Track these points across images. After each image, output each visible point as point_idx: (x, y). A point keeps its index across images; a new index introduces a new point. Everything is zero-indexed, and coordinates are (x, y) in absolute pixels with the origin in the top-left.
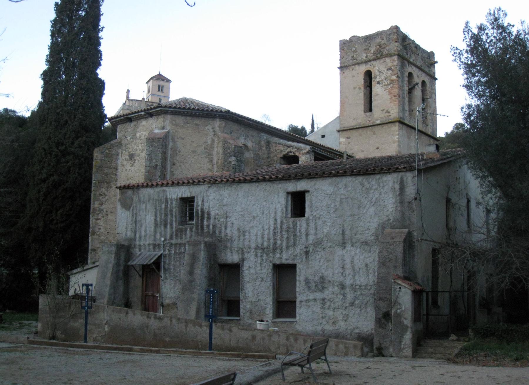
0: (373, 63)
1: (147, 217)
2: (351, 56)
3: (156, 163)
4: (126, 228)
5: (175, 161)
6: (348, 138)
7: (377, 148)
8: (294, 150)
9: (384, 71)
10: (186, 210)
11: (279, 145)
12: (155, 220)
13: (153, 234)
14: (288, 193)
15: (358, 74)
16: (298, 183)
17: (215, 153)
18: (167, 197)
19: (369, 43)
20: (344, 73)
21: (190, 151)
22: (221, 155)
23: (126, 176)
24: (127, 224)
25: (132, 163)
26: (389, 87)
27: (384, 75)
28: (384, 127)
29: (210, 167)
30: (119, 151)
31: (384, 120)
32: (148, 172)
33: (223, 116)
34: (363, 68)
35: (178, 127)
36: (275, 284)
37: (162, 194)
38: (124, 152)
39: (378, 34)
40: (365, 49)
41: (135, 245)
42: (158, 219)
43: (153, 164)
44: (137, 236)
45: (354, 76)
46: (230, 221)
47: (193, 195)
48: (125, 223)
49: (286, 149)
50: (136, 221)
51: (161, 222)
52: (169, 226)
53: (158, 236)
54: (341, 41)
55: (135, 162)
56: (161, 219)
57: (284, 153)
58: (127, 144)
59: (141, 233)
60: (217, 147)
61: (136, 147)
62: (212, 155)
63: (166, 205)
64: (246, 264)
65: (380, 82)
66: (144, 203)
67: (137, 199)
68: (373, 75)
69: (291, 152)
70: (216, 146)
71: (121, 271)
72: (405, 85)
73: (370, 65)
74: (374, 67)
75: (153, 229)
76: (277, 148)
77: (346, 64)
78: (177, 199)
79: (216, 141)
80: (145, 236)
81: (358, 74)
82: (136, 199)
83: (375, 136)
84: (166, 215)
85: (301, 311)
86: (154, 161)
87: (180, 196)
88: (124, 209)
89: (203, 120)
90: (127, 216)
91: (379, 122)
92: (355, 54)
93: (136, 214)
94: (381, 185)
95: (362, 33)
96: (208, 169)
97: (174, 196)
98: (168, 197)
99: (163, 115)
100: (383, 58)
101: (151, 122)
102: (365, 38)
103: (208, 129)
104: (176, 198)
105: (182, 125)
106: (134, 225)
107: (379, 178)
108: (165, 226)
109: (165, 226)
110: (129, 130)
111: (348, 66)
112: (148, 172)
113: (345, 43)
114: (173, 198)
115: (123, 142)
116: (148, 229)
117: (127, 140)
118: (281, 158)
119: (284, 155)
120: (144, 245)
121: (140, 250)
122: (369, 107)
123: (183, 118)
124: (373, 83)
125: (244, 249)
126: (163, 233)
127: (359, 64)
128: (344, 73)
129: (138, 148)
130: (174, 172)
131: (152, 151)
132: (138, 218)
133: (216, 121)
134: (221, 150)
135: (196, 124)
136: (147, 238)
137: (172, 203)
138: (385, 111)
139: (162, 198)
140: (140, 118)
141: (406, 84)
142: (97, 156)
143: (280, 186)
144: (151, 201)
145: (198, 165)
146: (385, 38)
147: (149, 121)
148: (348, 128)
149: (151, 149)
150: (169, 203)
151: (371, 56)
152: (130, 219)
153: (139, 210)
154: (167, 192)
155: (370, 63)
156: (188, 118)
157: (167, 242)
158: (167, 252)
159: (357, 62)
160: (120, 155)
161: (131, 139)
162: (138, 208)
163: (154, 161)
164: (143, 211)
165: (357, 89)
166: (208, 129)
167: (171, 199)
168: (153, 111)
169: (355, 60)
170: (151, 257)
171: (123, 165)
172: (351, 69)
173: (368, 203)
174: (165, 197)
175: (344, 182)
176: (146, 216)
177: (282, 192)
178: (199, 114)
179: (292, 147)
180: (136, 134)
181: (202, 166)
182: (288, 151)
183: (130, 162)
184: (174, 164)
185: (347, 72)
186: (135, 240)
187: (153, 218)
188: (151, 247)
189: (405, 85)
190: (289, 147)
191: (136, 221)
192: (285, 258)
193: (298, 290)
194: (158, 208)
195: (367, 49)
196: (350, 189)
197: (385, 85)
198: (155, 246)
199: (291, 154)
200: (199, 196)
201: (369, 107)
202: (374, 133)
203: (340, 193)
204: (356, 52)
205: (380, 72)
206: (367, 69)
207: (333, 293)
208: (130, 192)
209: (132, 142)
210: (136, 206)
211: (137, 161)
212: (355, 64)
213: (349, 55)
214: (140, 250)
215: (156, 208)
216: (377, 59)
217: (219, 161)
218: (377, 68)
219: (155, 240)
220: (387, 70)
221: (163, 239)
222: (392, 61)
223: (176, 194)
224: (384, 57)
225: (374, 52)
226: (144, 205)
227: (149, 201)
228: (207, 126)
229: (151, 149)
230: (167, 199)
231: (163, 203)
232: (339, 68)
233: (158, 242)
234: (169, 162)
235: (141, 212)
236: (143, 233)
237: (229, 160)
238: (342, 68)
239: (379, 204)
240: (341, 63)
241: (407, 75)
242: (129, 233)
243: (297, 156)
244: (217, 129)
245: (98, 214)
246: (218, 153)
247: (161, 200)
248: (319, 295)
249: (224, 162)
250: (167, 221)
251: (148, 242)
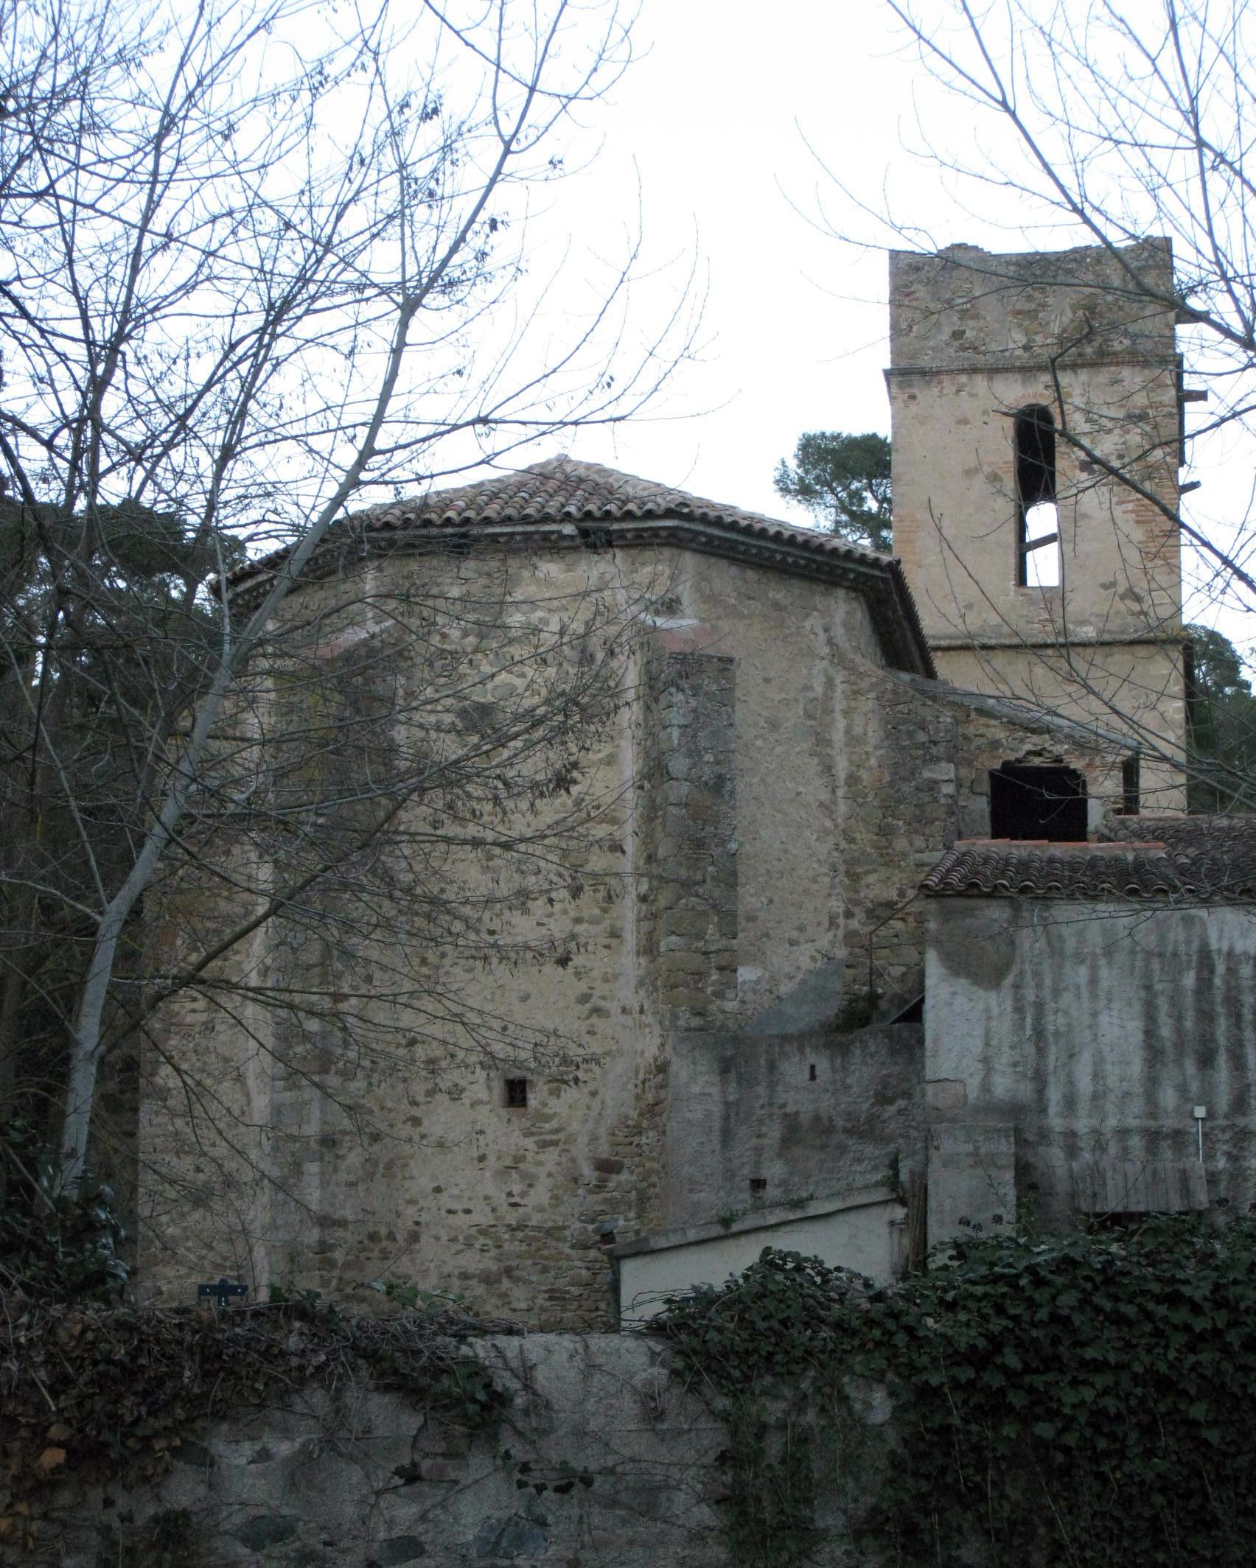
1: (1104, 1019)
3: (718, 769)
4: (986, 1060)
8: (1060, 749)
11: (983, 720)
12: (1150, 1033)
13: (1138, 1089)
17: (838, 735)
21: (762, 723)
22: (876, 747)
24: (987, 1044)
28: (1117, 657)
29: (824, 796)
31: (1114, 625)
32: (687, 805)
37: (1180, 930)
39: (1084, 258)
40: (1020, 312)
41: (1044, 1135)
42: (1166, 1031)
43: (707, 773)
44: (1054, 1095)
45: (964, 421)
48: (979, 1043)
49: (1022, 741)
50: (1039, 1034)
51: (1180, 1045)
52: (1222, 1060)
53: (1168, 1097)
56: (1179, 1030)
57: (1012, 757)
59: (1071, 1082)
60: (846, 713)
62: (828, 743)
63: (1206, 974)
66: (1082, 962)
67: (1041, 944)
69: (1039, 754)
70: (839, 705)
75: (1137, 1068)
76: (971, 730)
77: (925, 361)
79: (840, 688)
80: (1095, 1097)
82: (1030, 942)
84: (1206, 1016)
86: (709, 757)
88: (963, 982)
89: (798, 587)
90: (987, 1009)
91: (1089, 632)
92: (972, 323)
93: (1039, 1006)
96: (822, 804)
98: (1214, 945)
99: (667, 553)
100: (1110, 364)
101: (595, 573)
102: (1017, 264)
106: (1030, 1050)
108: (1206, 1060)
109: (1206, 1060)
111: (939, 373)
112: (687, 805)
113: (918, 269)
116: (1109, 1067)
118: (992, 774)
119: (1006, 764)
120: (1097, 1132)
121: (1072, 1152)
123: (734, 570)
126: (1194, 1087)
127: (993, 371)
128: (913, 397)
131: (694, 711)
132: (1054, 1022)
134: (873, 733)
135: (777, 606)
136: (1110, 1107)
137: (1232, 971)
138: (1121, 588)
139: (1182, 948)
140: (551, 546)
144: (1121, 957)
145: (790, 785)
147: (583, 566)
148: (944, 643)
149: (693, 703)
150: (1221, 968)
151: (1045, 345)
152: (1004, 1028)
153: (1057, 992)
154: (1203, 924)
156: (751, 574)
157: (1221, 1122)
158: (1222, 1163)
159: (981, 360)
162: (1048, 982)
163: (709, 757)
164: (1078, 997)
165: (980, 478)
167: (1230, 954)
169: (969, 354)
174: (1195, 945)
176: (1095, 1015)
178: (795, 564)
179: (1049, 731)
181: (801, 789)
182: (1028, 747)
185: (928, 395)
186: (1043, 1110)
187: (1135, 1027)
188: (1136, 1142)
190: (1033, 731)
191: (1039, 1034)
194: (1158, 987)
195: (1032, 314)
198: (1153, 1138)
199: (1037, 761)
204: (976, 317)
206: (1033, 401)
208: (996, 913)
210: (1037, 974)
212: (974, 370)
213: (938, 325)
214: (1072, 1152)
215: (1148, 988)
216: (1083, 366)
217: (864, 774)
219: (1152, 1115)
221: (1200, 1112)
224: (1117, 364)
225: (1064, 330)
226: (1083, 972)
228: (808, 615)
229: (693, 703)
231: (1189, 968)
233: (1169, 1123)
235: (1067, 998)
236: (1085, 1085)
237: (926, 774)
240: (896, 353)
242: (1003, 1085)
243: (1074, 771)
244: (839, 632)
245: (339, 976)
246: (853, 740)
247: (1175, 954)
249: (891, 784)
250: (1213, 1039)
251: (1112, 1122)
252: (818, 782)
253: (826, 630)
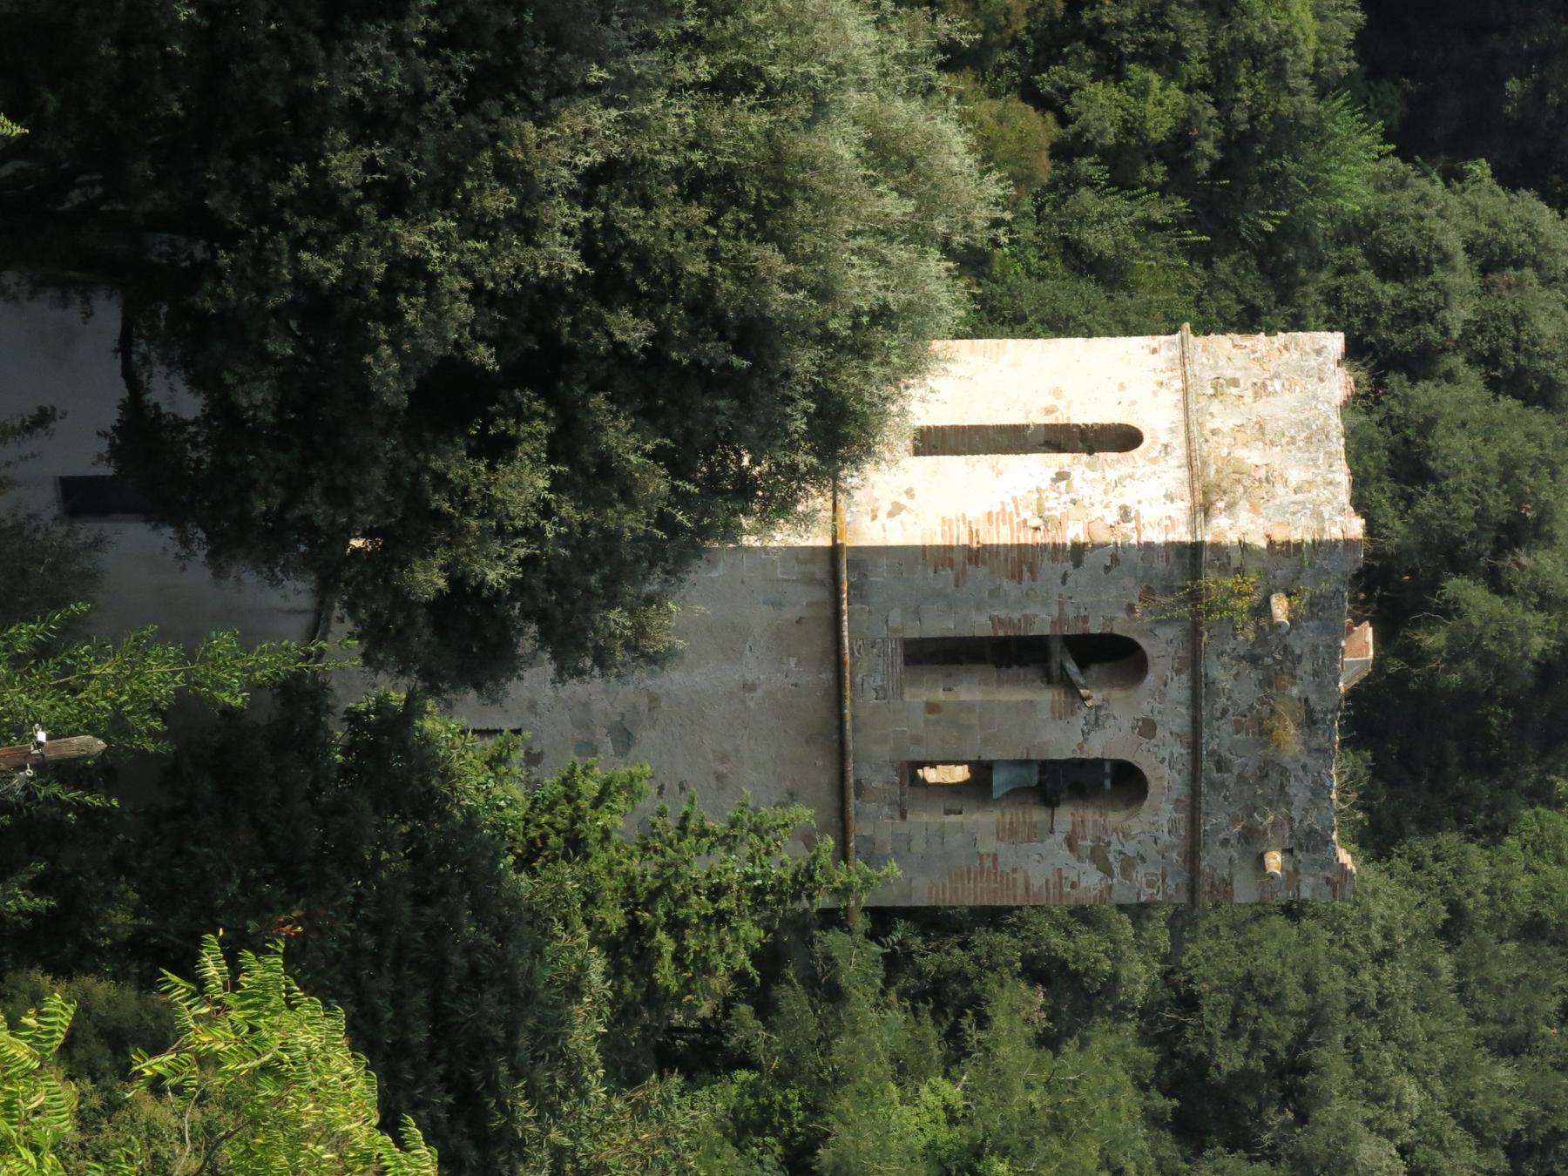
2: (1239, 375)
15: (1133, 403)
19: (1293, 441)
27: (1097, 495)
45: (1122, 387)
65: (1063, 485)
146: (1300, 497)
165: (1051, 401)
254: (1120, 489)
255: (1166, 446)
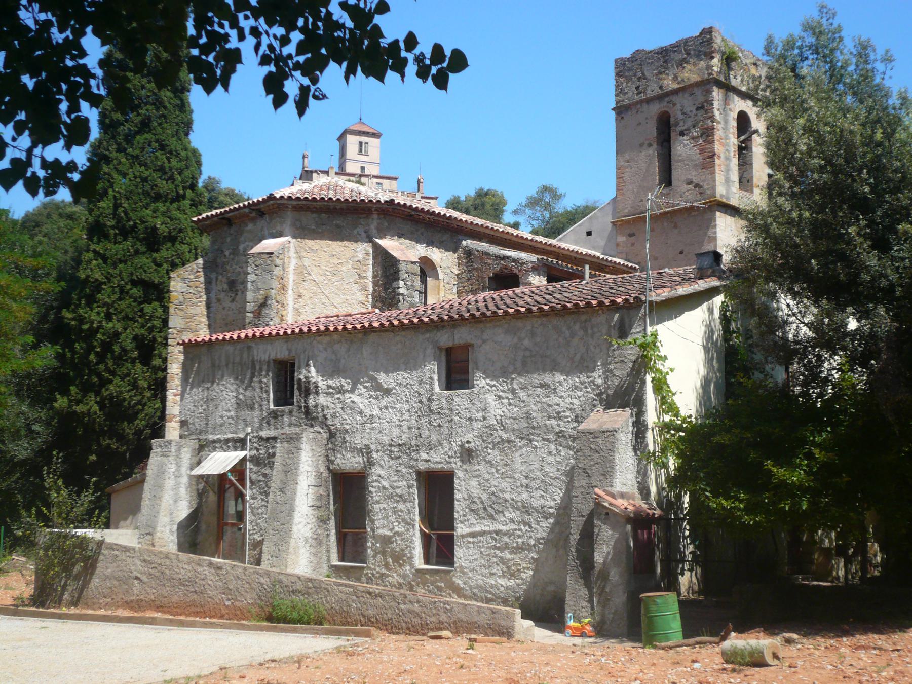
0: (674, 98)
2: (634, 87)
5: (301, 291)
6: (631, 235)
7: (681, 253)
9: (691, 111)
10: (286, 380)
14: (440, 349)
16: (456, 332)
18: (253, 358)
20: (622, 118)
23: (224, 319)
25: (233, 295)
26: (701, 141)
27: (692, 119)
30: (212, 276)
33: (383, 210)
34: (655, 109)
35: (306, 232)
36: (423, 507)
38: (220, 277)
39: (680, 45)
45: (639, 124)
46: (350, 398)
47: (293, 354)
54: (616, 61)
55: (237, 295)
58: (224, 263)
61: (239, 269)
64: (376, 471)
65: (685, 132)
68: (672, 120)
71: (183, 486)
72: (731, 136)
73: (668, 102)
74: (674, 105)
78: (268, 362)
81: (647, 118)
83: (676, 231)
85: (460, 553)
87: (273, 356)
94: (590, 331)
95: (652, 44)
97: (265, 357)
98: (256, 358)
102: (658, 53)
103: (358, 233)
104: (267, 359)
105: (313, 227)
107: (586, 321)
110: (228, 240)
114: (263, 358)
115: (219, 261)
117: (225, 256)
122: (667, 179)
123: (315, 215)
124: (673, 135)
125: (371, 446)
127: (649, 101)
128: (622, 118)
129: (240, 270)
130: (300, 311)
133: (373, 220)
135: (338, 226)
141: (733, 133)
142: (174, 286)
143: (428, 335)
144: (230, 366)
155: (667, 99)
157: (255, 434)
160: (214, 282)
161: (230, 254)
166: (358, 233)
167: (260, 362)
168: (262, 206)
170: (230, 460)
171: (219, 300)
172: (634, 111)
173: (568, 365)
174: (251, 358)
175: (529, 328)
177: (431, 346)
180: (238, 247)
181: (348, 298)
183: (230, 294)
184: (300, 296)
185: (628, 117)
189: (731, 136)
192: (436, 459)
193: (456, 515)
196: (538, 339)
197: (693, 138)
200: (302, 357)
201: (667, 179)
202: (676, 227)
203: (523, 347)
205: (684, 114)
207: (512, 521)
209: (233, 259)
211: (239, 293)
218: (678, 107)
220: (697, 110)
222: (704, 93)
223: (268, 353)
227: (227, 365)
228: (356, 228)
230: (253, 361)
232: (613, 109)
234: (290, 292)
238: (621, 110)
239: (585, 364)
241: (736, 117)
248: (488, 526)
252: (359, 294)
253: (365, 232)
254: (688, 113)
255: (668, 102)
